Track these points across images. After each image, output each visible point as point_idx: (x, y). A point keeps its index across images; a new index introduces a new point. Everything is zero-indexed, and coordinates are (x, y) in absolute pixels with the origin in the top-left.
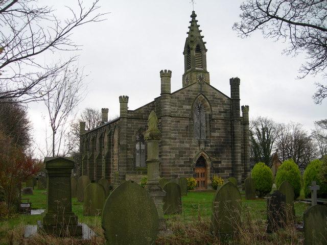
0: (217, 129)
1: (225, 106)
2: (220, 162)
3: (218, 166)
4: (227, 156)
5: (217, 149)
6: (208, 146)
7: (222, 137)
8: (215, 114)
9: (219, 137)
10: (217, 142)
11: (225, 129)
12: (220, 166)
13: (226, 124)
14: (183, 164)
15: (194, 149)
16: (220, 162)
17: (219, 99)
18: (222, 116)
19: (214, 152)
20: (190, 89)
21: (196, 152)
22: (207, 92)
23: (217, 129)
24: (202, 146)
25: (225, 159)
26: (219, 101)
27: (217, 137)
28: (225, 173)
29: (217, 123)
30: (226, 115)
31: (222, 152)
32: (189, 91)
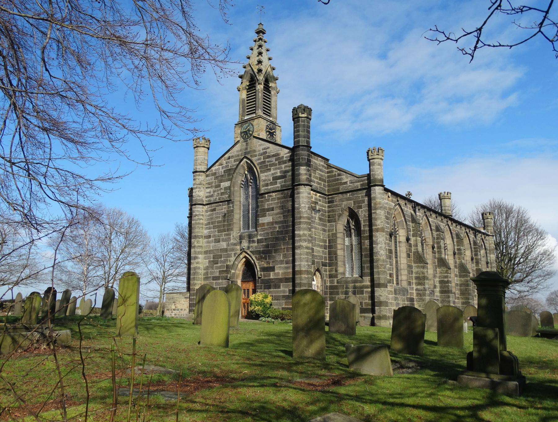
0: (268, 210)
1: (283, 166)
2: (273, 269)
3: (269, 275)
4: (285, 256)
5: (267, 246)
6: (253, 242)
7: (276, 223)
8: (267, 185)
9: (272, 223)
10: (268, 233)
11: (282, 207)
12: (272, 276)
13: (284, 197)
14: (217, 274)
15: (233, 250)
16: (273, 269)
17: (273, 156)
18: (278, 185)
19: (263, 252)
20: (231, 155)
21: (235, 254)
22: (255, 151)
23: (268, 210)
24: (245, 244)
25: (281, 262)
26: (273, 159)
27: (268, 224)
28: (282, 289)
29: (268, 200)
30: (285, 181)
31: (276, 251)
32: (229, 158)
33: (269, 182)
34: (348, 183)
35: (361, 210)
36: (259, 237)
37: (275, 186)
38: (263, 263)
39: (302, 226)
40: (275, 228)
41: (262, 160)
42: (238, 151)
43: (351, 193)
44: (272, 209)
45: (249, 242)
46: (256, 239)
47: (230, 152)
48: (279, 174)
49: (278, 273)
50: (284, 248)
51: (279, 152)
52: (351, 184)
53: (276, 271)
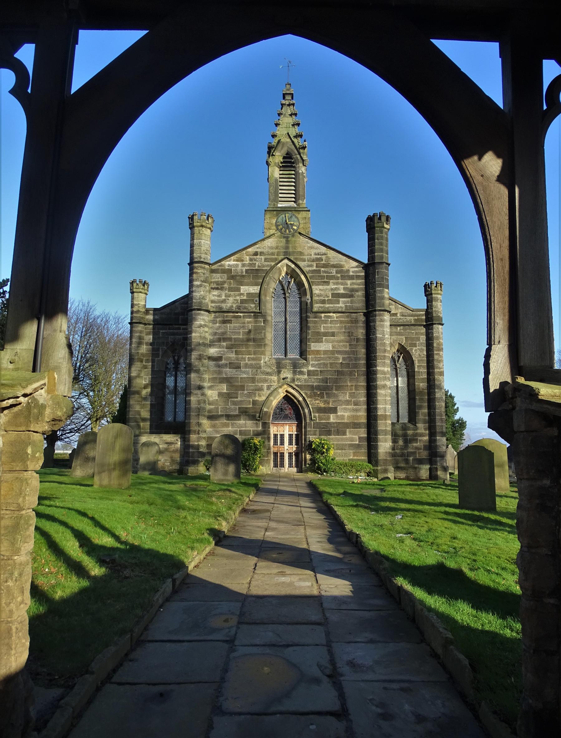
0: (326, 334)
1: (349, 282)
2: (334, 410)
3: (329, 418)
4: (352, 395)
5: (325, 380)
6: (301, 373)
7: (339, 352)
8: (323, 302)
9: (333, 352)
10: (325, 365)
11: (350, 334)
12: (332, 418)
13: (352, 322)
15: (266, 381)
16: (334, 410)
17: (334, 266)
18: (342, 304)
19: (318, 388)
20: (259, 250)
21: (269, 388)
22: (301, 253)
23: (326, 334)
24: (287, 374)
25: (348, 403)
26: (334, 271)
27: (325, 352)
28: (348, 435)
29: (326, 322)
30: (352, 302)
31: (338, 388)
32: (256, 254)
33: (326, 299)
34: (398, 315)
35: (414, 348)
36: (311, 368)
37: (335, 305)
38: (317, 402)
39: (386, 361)
40: (337, 358)
41: (315, 268)
42: (272, 248)
43: (402, 327)
44: (333, 334)
45: (295, 373)
46: (305, 370)
47: (257, 246)
48: (342, 291)
49: (343, 416)
50: (352, 386)
51: (342, 263)
52: (402, 317)
53: (339, 414)
